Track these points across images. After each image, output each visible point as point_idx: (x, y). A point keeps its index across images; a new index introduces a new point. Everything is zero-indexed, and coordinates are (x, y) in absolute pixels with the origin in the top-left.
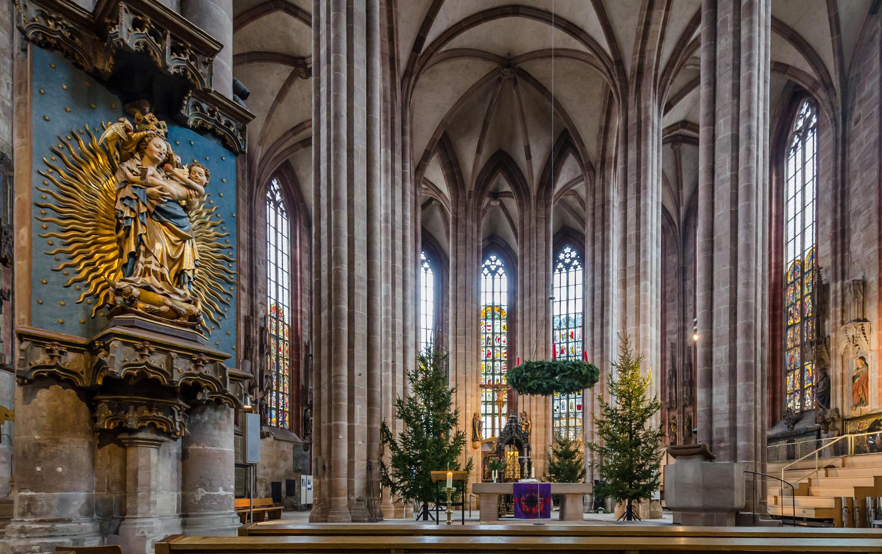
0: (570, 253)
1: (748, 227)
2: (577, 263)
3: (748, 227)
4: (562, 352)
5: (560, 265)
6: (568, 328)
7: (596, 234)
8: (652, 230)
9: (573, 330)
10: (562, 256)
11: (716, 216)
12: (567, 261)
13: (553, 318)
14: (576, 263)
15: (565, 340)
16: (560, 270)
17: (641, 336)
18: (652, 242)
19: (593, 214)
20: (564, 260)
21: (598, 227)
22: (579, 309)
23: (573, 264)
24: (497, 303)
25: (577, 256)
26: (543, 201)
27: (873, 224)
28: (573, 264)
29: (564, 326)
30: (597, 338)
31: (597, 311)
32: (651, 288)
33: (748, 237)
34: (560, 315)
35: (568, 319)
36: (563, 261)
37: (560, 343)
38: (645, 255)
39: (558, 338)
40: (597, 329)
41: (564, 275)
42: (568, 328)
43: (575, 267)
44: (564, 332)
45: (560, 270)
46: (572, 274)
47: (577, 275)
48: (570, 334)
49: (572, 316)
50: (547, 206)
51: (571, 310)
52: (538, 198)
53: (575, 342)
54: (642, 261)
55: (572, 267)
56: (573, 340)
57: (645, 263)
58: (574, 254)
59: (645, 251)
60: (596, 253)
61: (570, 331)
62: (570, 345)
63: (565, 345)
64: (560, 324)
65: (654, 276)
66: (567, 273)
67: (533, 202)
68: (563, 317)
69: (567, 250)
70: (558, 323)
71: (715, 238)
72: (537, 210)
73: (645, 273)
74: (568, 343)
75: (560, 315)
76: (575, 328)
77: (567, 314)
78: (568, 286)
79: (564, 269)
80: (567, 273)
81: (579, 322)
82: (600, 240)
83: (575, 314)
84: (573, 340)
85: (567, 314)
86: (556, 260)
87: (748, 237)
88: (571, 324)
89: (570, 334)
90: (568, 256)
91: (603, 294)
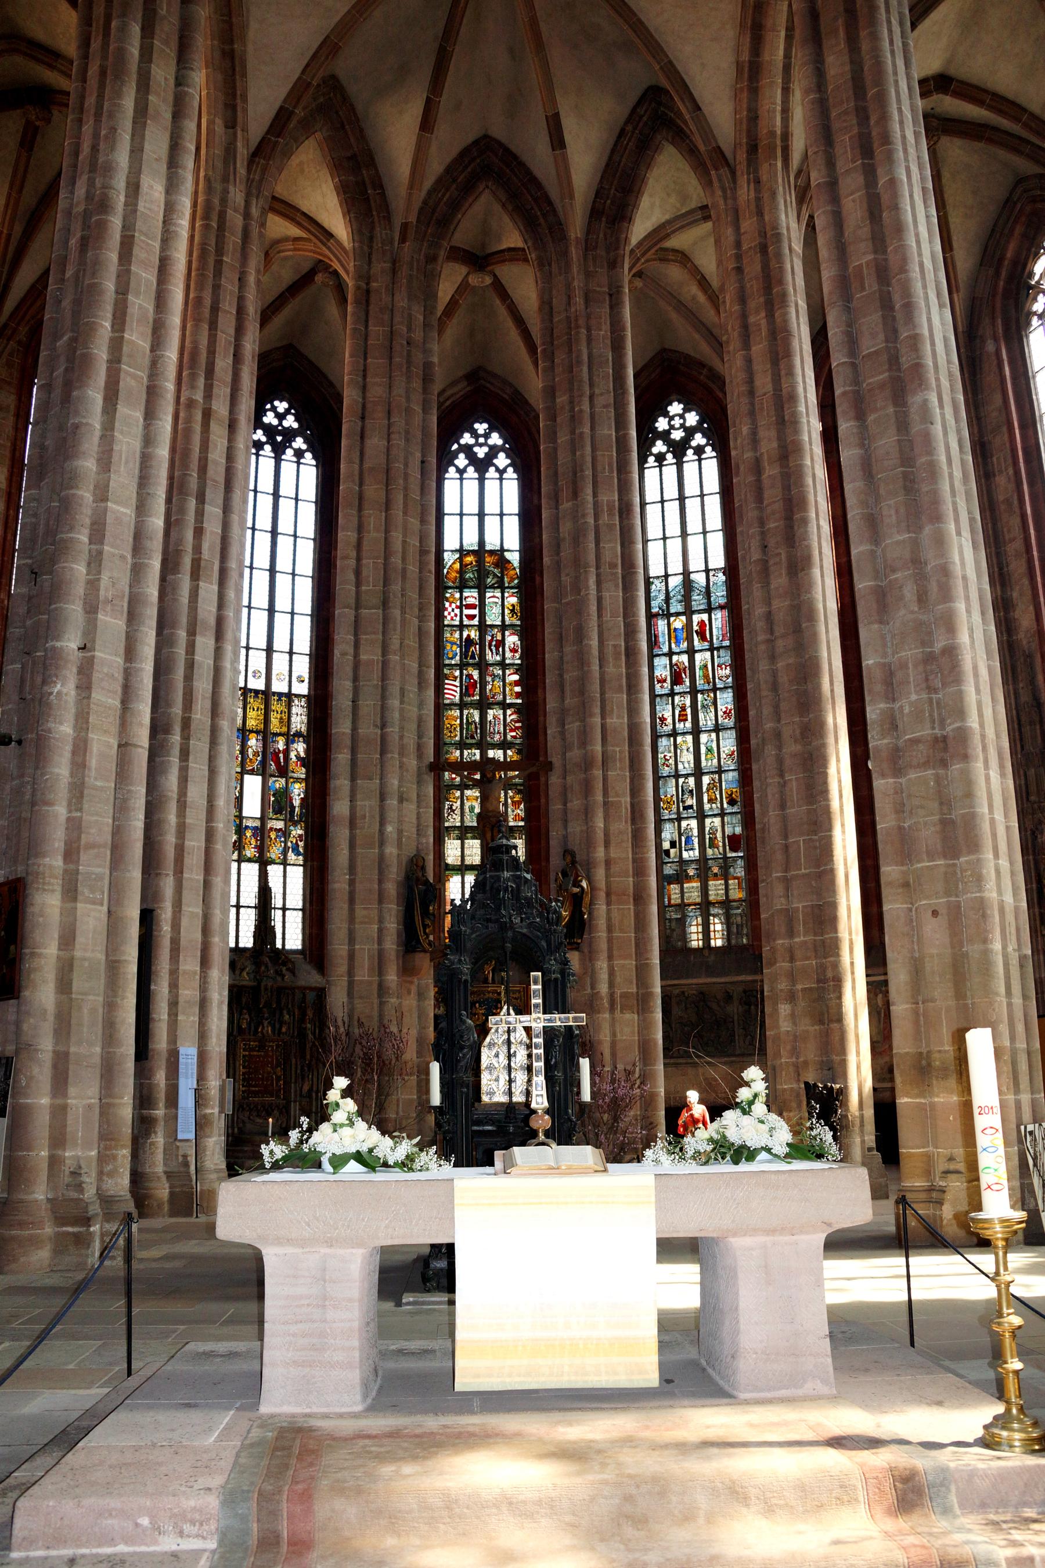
0: (682, 416)
2: (703, 441)
4: (677, 679)
5: (659, 447)
6: (689, 612)
7: (752, 319)
8: (920, 255)
9: (705, 617)
10: (662, 424)
12: (677, 435)
13: (648, 583)
14: (699, 439)
15: (684, 645)
16: (660, 458)
20: (667, 433)
21: (756, 301)
22: (718, 560)
23: (694, 443)
24: (492, 542)
25: (700, 422)
26: (601, 252)
28: (694, 443)
29: (676, 607)
32: (943, 415)
34: (666, 576)
35: (688, 584)
36: (665, 436)
37: (670, 654)
39: (663, 639)
41: (670, 472)
42: (689, 612)
43: (699, 451)
44: (679, 623)
45: (660, 458)
46: (690, 469)
48: (696, 628)
49: (700, 579)
50: (614, 264)
51: (696, 563)
52: (588, 246)
53: (711, 649)
55: (690, 452)
56: (706, 645)
58: (692, 419)
60: (757, 367)
61: (696, 618)
62: (698, 657)
63: (684, 658)
64: (667, 599)
66: (680, 465)
67: (574, 253)
68: (675, 582)
69: (676, 408)
70: (662, 597)
72: (588, 275)
74: (691, 652)
75: (666, 576)
76: (709, 610)
77: (686, 573)
78: (682, 499)
79: (669, 456)
80: (680, 465)
81: (719, 595)
82: (764, 332)
83: (707, 571)
84: (706, 645)
85: (686, 573)
86: (647, 435)
88: (698, 600)
89: (696, 628)
90: (677, 422)
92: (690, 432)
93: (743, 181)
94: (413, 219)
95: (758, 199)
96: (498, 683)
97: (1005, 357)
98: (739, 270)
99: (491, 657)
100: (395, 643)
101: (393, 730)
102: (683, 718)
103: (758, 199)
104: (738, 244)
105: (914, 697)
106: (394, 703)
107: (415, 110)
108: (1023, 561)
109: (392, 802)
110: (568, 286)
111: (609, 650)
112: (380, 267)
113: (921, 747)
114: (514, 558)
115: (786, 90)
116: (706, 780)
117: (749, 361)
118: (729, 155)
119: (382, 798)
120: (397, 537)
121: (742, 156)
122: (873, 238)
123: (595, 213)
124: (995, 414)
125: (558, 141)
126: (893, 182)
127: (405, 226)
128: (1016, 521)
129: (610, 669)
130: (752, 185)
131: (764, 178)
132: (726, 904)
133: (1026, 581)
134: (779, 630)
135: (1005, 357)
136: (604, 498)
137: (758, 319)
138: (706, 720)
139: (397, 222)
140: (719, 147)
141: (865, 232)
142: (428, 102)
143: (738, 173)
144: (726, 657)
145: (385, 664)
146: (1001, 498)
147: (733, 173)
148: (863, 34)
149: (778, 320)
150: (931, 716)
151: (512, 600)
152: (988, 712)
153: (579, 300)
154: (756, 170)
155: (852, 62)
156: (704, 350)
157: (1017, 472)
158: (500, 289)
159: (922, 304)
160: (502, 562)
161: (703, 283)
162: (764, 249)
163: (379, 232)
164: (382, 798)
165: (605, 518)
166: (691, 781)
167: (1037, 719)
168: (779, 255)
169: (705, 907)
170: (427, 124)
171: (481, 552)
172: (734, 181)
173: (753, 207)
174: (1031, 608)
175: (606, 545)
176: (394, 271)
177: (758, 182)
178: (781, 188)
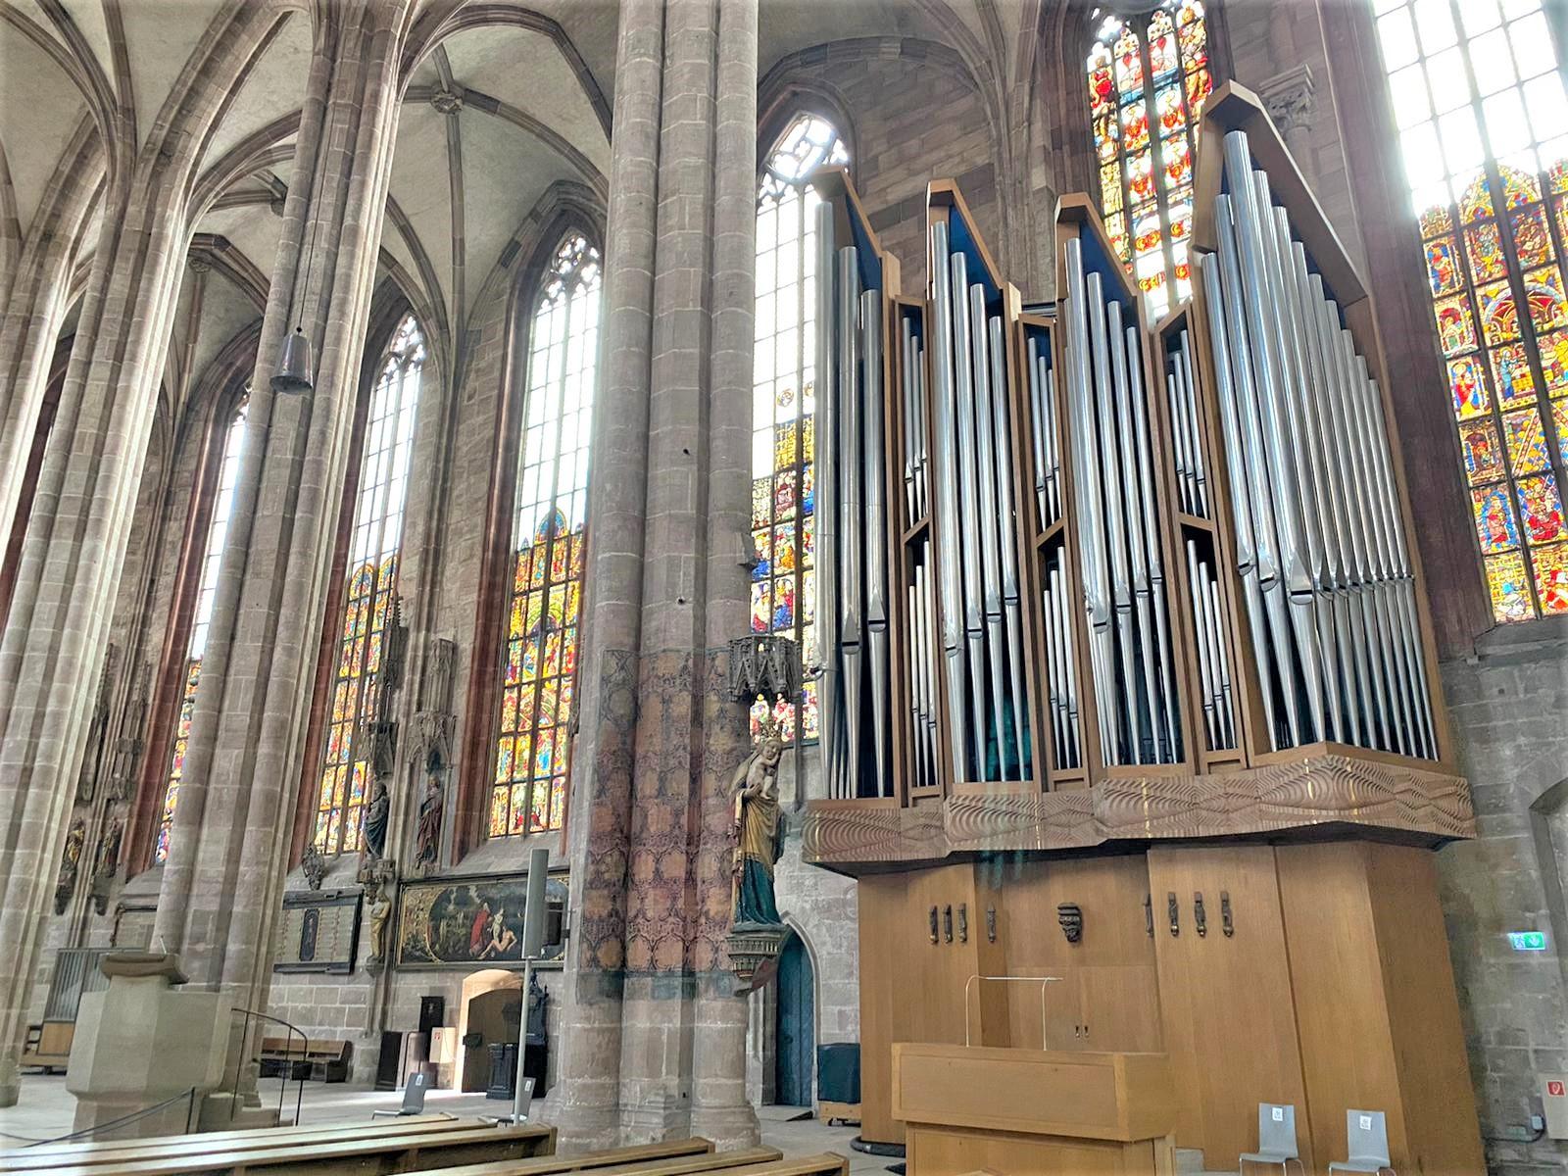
1: (304, 554)
3: (304, 554)
8: (130, 441)
11: (259, 514)
17: (62, 654)
18: (126, 464)
27: (475, 560)
32: (106, 556)
38: (106, 488)
54: (97, 495)
57: (103, 503)
59: (108, 478)
65: (117, 532)
71: (252, 550)
73: (99, 521)
87: (302, 571)
93: (28, 257)
95: (37, 281)
97: (209, 436)
103: (37, 281)
105: (19, 738)
108: (170, 594)
113: (13, 772)
115: (91, 208)
118: (24, 231)
122: (101, 419)
124: (187, 474)
126: (127, 389)
128: (176, 562)
130: (35, 266)
131: (47, 267)
133: (167, 609)
135: (209, 436)
140: (17, 220)
141: (98, 410)
143: (27, 250)
146: (170, 539)
147: (22, 247)
148: (145, 275)
149: (17, 388)
150: (27, 754)
152: (70, 756)
154: (43, 257)
155: (131, 287)
157: (187, 526)
159: (119, 480)
167: (140, 715)
168: (36, 336)
172: (21, 254)
173: (30, 284)
174: (164, 630)
177: (41, 266)
178: (59, 282)
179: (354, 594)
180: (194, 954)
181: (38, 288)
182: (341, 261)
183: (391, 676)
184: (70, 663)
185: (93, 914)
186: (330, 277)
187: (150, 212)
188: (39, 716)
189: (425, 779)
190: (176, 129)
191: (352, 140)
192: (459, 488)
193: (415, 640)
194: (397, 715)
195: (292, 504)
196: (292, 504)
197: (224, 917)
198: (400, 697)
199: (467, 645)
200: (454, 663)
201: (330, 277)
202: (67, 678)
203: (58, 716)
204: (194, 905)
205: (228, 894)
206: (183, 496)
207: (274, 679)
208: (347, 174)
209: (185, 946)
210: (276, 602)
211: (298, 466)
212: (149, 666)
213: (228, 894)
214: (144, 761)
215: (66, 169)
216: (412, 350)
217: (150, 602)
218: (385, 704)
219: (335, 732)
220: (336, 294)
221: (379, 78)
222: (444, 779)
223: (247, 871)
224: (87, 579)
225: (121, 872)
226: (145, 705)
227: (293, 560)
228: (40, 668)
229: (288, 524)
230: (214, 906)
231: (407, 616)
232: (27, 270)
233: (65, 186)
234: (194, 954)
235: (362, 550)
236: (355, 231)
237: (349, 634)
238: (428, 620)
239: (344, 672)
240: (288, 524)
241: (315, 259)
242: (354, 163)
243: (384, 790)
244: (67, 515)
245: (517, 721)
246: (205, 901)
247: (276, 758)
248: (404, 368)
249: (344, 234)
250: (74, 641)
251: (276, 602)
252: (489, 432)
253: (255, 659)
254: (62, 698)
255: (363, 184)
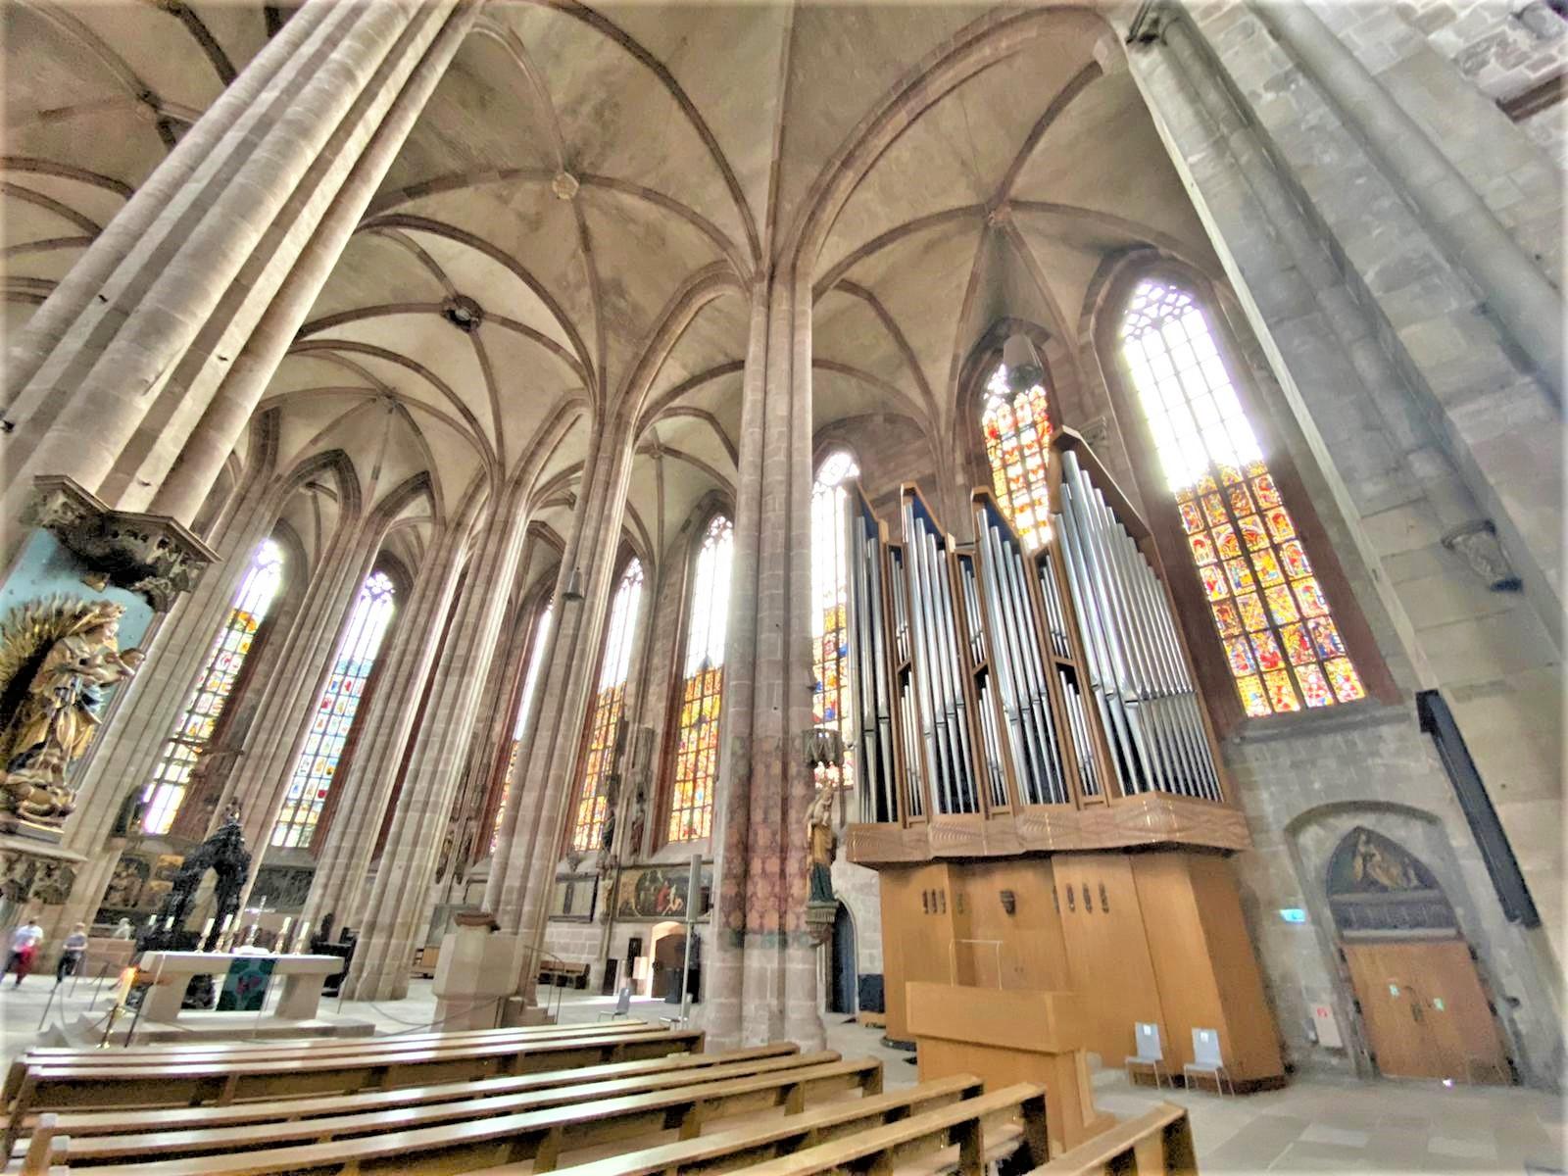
4: (325, 705)
6: (346, 674)
9: (352, 680)
12: (377, 591)
15: (336, 690)
19: (432, 570)
21: (433, 586)
30: (390, 714)
31: (401, 680)
33: (575, 692)
35: (350, 662)
38: (477, 650)
40: (393, 704)
42: (346, 674)
43: (385, 601)
47: (386, 610)
49: (357, 661)
50: (378, 533)
52: (369, 521)
57: (476, 658)
59: (479, 644)
61: (347, 679)
62: (341, 698)
67: (361, 523)
73: (472, 668)
74: (338, 694)
87: (575, 692)
88: (352, 671)
91: (414, 662)
92: (384, 591)
94: (286, 475)
96: (218, 681)
98: (432, 570)
99: (219, 666)
100: (180, 672)
101: (157, 718)
102: (320, 725)
104: (435, 559)
106: (164, 703)
107: (314, 433)
109: (139, 756)
110: (352, 534)
111: (298, 705)
112: (257, 489)
114: (258, 620)
116: (319, 759)
117: (419, 609)
119: (134, 751)
120: (203, 624)
121: (453, 525)
123: (379, 508)
125: (376, 475)
127: (279, 478)
129: (295, 715)
132: (304, 825)
134: (384, 724)
136: (326, 636)
137: (430, 594)
138: (331, 730)
139: (278, 471)
141: (477, 609)
142: (320, 434)
144: (356, 702)
145: (167, 684)
151: (248, 639)
153: (354, 543)
156: (406, 560)
158: (315, 498)
160: (249, 620)
161: (418, 538)
162: (445, 567)
163: (265, 472)
164: (134, 751)
165: (323, 645)
166: (311, 758)
169: (291, 825)
170: (315, 441)
171: (238, 611)
175: (318, 657)
176: (264, 493)
179: (602, 703)
180: (505, 912)
181: (452, 550)
182: (602, 532)
183: (619, 748)
184: (452, 743)
185: (455, 883)
186: (596, 541)
187: (509, 511)
188: (434, 773)
189: (635, 807)
190: (524, 471)
191: (609, 474)
192: (658, 645)
193: (632, 728)
194: (622, 771)
195: (571, 657)
196: (571, 657)
197: (522, 891)
198: (623, 760)
199: (660, 730)
200: (652, 741)
201: (596, 541)
202: (450, 752)
203: (444, 773)
204: (507, 884)
205: (525, 878)
206: (516, 652)
207: (556, 753)
208: (606, 490)
209: (501, 908)
210: (560, 710)
211: (575, 637)
212: (493, 744)
213: (525, 878)
214: (487, 796)
215: (470, 491)
216: (635, 575)
217: (495, 710)
218: (615, 764)
219: (588, 780)
220: (599, 549)
221: (624, 443)
222: (645, 807)
223: (536, 863)
224: (464, 698)
225: (471, 860)
226: (489, 765)
227: (570, 687)
228: (437, 746)
229: (569, 667)
230: (517, 884)
231: (629, 714)
232: (447, 540)
233: (469, 499)
234: (505, 912)
235: (607, 682)
236: (609, 517)
237: (598, 724)
238: (640, 717)
239: (594, 746)
240: (569, 667)
241: (588, 532)
242: (609, 485)
243: (613, 814)
244: (457, 664)
245: (685, 774)
246: (513, 881)
247: (555, 797)
248: (631, 584)
249: (604, 518)
250: (455, 732)
251: (560, 710)
252: (674, 616)
253: (547, 742)
254: (447, 764)
255: (614, 495)
